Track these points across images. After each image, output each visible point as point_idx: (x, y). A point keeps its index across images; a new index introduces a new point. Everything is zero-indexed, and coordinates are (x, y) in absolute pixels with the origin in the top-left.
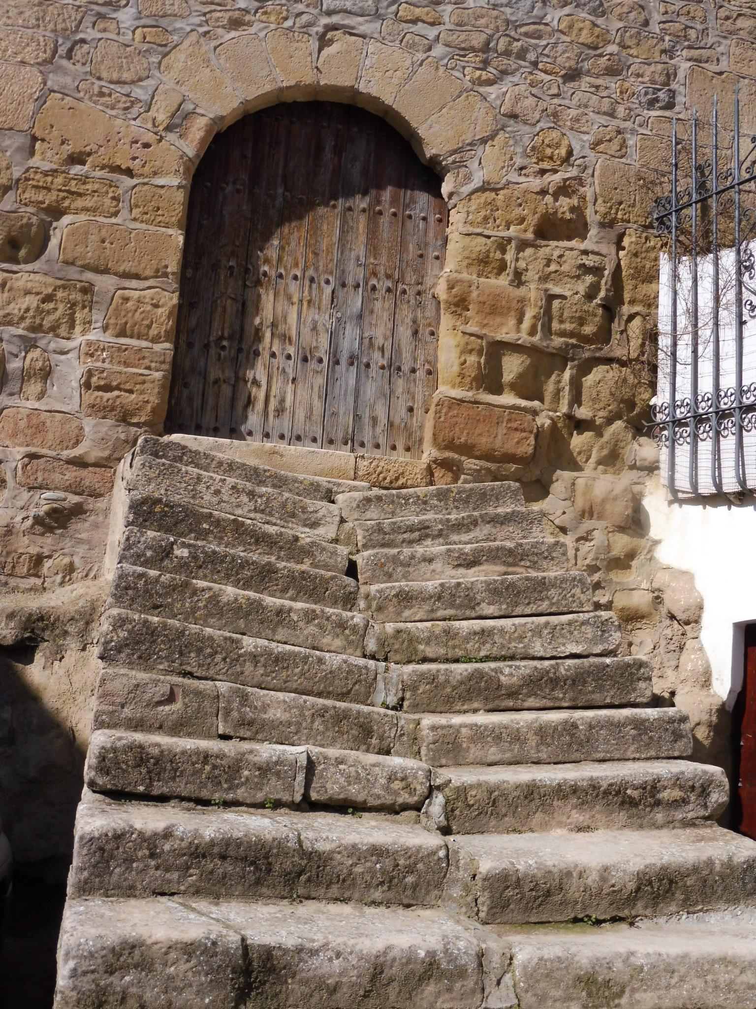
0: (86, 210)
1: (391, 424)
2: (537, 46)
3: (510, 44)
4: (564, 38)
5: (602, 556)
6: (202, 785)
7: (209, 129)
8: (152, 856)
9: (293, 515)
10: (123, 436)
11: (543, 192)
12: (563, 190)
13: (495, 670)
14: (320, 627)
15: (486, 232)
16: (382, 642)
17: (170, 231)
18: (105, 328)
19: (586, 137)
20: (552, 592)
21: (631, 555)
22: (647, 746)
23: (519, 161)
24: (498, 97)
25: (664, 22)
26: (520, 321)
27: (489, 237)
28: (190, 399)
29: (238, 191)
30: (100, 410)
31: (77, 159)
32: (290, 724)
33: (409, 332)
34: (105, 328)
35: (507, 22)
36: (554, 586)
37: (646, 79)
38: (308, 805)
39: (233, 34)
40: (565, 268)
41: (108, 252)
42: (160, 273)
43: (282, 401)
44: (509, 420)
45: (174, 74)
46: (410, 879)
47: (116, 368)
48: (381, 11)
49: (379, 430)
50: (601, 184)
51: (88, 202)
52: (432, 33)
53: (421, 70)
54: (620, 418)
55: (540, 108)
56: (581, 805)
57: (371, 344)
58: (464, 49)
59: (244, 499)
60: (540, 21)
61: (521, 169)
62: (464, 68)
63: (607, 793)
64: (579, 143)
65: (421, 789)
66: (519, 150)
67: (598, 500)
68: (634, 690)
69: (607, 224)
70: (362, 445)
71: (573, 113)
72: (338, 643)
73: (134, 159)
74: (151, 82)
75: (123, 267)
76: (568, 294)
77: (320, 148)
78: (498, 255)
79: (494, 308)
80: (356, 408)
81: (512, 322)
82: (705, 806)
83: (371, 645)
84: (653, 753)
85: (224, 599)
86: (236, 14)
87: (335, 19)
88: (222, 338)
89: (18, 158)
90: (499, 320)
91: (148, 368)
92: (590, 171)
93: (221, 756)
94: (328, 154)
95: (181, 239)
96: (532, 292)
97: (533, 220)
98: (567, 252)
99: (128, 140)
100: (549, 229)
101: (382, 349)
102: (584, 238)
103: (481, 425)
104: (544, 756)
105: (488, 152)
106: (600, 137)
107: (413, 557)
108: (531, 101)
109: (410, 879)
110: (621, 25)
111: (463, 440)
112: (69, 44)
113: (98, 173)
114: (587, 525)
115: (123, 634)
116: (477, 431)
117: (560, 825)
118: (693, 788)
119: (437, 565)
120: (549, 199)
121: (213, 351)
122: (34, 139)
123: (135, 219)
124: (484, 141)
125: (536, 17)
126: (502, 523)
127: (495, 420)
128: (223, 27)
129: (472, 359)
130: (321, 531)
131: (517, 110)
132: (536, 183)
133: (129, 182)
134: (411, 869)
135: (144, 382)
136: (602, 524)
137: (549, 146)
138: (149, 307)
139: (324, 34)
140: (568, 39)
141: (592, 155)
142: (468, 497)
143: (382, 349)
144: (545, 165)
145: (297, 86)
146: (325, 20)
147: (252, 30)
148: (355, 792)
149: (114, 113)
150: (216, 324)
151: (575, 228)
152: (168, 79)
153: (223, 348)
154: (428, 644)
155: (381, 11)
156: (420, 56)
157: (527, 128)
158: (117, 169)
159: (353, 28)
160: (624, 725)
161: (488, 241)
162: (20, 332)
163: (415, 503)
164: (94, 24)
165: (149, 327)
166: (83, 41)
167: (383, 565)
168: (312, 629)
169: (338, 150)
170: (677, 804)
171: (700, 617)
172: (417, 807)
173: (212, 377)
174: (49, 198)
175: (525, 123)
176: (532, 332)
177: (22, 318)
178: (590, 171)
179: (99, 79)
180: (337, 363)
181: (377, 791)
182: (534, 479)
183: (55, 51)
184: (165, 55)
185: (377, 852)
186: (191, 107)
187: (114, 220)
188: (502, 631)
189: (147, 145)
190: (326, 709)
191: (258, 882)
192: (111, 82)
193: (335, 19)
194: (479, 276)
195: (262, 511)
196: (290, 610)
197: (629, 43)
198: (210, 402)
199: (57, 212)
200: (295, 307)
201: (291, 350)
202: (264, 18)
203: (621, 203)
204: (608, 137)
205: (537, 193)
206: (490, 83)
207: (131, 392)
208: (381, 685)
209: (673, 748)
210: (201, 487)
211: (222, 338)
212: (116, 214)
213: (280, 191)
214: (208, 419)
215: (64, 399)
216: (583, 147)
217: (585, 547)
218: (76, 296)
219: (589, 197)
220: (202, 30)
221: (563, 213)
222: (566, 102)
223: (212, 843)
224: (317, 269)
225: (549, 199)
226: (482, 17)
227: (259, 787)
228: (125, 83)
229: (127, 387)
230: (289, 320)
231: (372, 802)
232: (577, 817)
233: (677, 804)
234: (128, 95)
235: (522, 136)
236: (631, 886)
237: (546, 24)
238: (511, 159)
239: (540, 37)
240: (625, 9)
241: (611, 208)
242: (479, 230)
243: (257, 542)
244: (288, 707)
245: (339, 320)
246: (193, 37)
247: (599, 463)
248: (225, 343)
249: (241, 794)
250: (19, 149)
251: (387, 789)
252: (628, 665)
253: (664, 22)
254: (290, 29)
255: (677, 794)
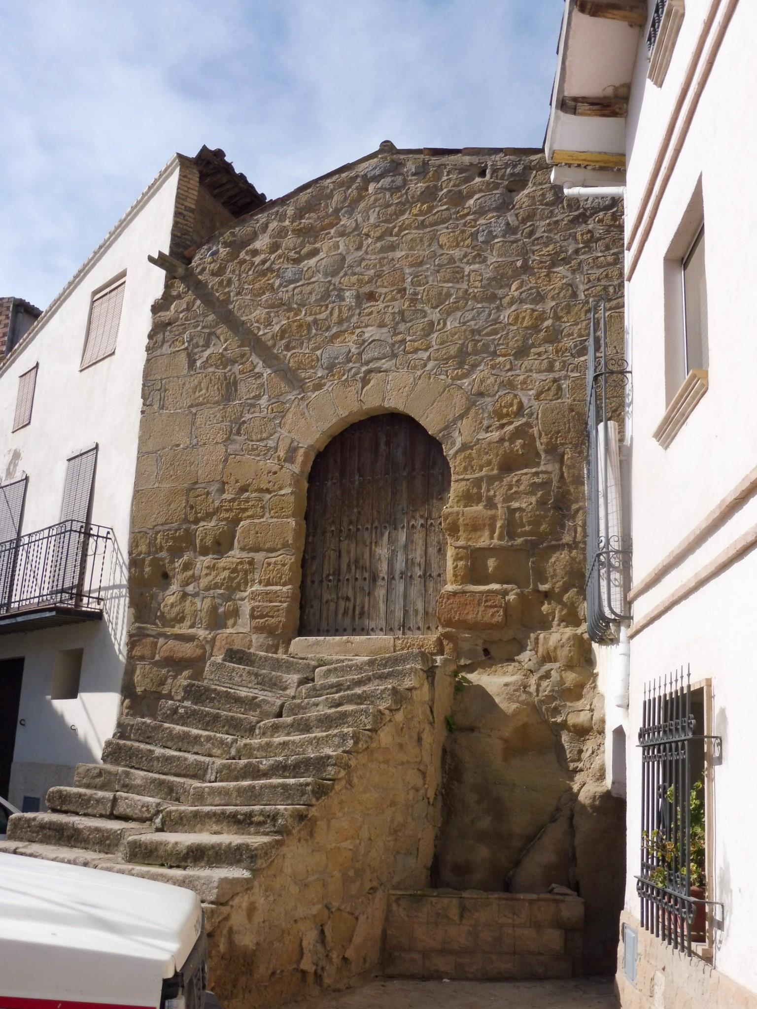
0: (249, 517)
1: (426, 613)
2: (494, 339)
3: (475, 345)
4: (512, 328)
5: (557, 688)
6: (78, 807)
7: (306, 455)
8: (29, 827)
9: (275, 685)
10: (271, 643)
11: (502, 440)
12: (519, 433)
13: (258, 762)
14: (213, 744)
15: (467, 477)
16: (238, 751)
17: (289, 520)
18: (260, 582)
19: (531, 393)
20: (350, 719)
21: (581, 686)
22: (288, 798)
23: (486, 423)
24: (469, 384)
25: (588, 290)
26: (492, 532)
27: (468, 480)
28: (314, 614)
29: (334, 484)
30: (258, 629)
31: (244, 489)
32: (141, 786)
33: (436, 550)
34: (260, 582)
35: (473, 332)
36: (351, 715)
37: (576, 335)
38: (112, 816)
39: (317, 393)
40: (522, 488)
41: (259, 539)
42: (285, 545)
43: (363, 608)
44: (486, 601)
45: (287, 427)
46: (108, 842)
47: (265, 604)
48: (396, 352)
49: (419, 618)
50: (543, 423)
51: (250, 513)
52: (425, 355)
53: (420, 382)
54: (574, 586)
55: (498, 382)
56: (218, 822)
57: (413, 563)
58: (446, 359)
59: (253, 678)
60: (496, 321)
61: (488, 427)
62: (447, 371)
63: (229, 816)
64: (526, 397)
65: (152, 811)
66: (486, 415)
67: (552, 648)
68: (325, 771)
69: (552, 450)
70: (409, 629)
71: (521, 378)
72: (219, 752)
73: (269, 482)
74: (277, 435)
75: (267, 546)
76: (524, 506)
77: (377, 445)
78: (475, 490)
79: (475, 527)
80: (405, 606)
81: (487, 533)
82: (274, 826)
83: (233, 752)
84: (290, 802)
85: (174, 732)
86: (317, 381)
87: (371, 365)
88: (329, 575)
89: (217, 496)
90: (479, 533)
91: (280, 602)
92: (535, 416)
93: (85, 795)
94: (383, 447)
95: (294, 523)
96: (500, 511)
97: (496, 461)
98: (525, 476)
99: (265, 473)
100: (508, 466)
101: (419, 565)
102: (538, 464)
103: (468, 607)
104: (238, 802)
105: (466, 425)
106: (540, 389)
107: (308, 704)
108: (492, 379)
109: (108, 842)
110: (554, 303)
111: (456, 618)
112: (238, 426)
113: (254, 495)
114: (548, 666)
115: (110, 749)
116: (466, 612)
117: (208, 830)
118: (269, 816)
119: (320, 707)
120: (507, 444)
121: (325, 583)
122: (224, 483)
123: (272, 517)
124: (461, 417)
125: (493, 320)
126: (386, 678)
127: (476, 602)
128: (311, 391)
129: (461, 564)
130: (288, 692)
131: (482, 389)
132: (495, 435)
133: (268, 496)
134: (108, 838)
135: (278, 610)
136: (557, 665)
137: (505, 407)
138: (279, 567)
139: (365, 377)
140: (515, 328)
141: (535, 403)
142: (387, 662)
143: (419, 565)
144: (504, 421)
145: (350, 414)
146: (364, 369)
147: (326, 388)
148: (129, 812)
149: (259, 458)
150: (326, 568)
151: (529, 458)
152: (284, 432)
153: (330, 581)
154: (258, 751)
155: (396, 352)
156: (419, 373)
157: (490, 399)
158: (261, 491)
159: (381, 368)
160: (278, 787)
161: (468, 483)
162: (222, 591)
163: (355, 670)
164: (249, 410)
165: (281, 578)
166: (244, 422)
167: (293, 709)
168: (209, 745)
169: (388, 443)
170: (261, 824)
171: (604, 729)
172: (150, 819)
173: (325, 599)
174: (231, 515)
175: (489, 395)
176: (501, 538)
177: (222, 584)
178: (535, 416)
179: (252, 441)
180: (393, 578)
181: (137, 811)
182: (511, 637)
183: (231, 432)
184: (283, 417)
185: (97, 830)
186: (296, 444)
187: (262, 520)
188: (294, 742)
189: (275, 473)
190: (155, 779)
191: (60, 839)
192: (258, 441)
193: (371, 365)
194: (465, 507)
195: (261, 684)
196: (201, 736)
197: (561, 314)
198: (324, 615)
199: (236, 521)
200: (368, 548)
201: (366, 575)
202: (331, 378)
203: (559, 432)
204: (546, 388)
205: (497, 442)
206: (465, 376)
207: (273, 617)
208: (209, 771)
209: (300, 800)
210: (234, 674)
211: (329, 575)
212: (262, 517)
213: (357, 477)
214: (324, 625)
215: (243, 626)
216: (530, 400)
217: (545, 684)
218: (246, 566)
219: (536, 435)
220: (299, 397)
221: (517, 450)
222: (518, 372)
223: (46, 823)
224: (379, 521)
225: (507, 444)
226: (456, 334)
227: (95, 808)
228: (264, 439)
229: (270, 614)
230: (365, 557)
231: (135, 816)
232: (215, 828)
233: (261, 824)
234: (266, 446)
235: (487, 405)
236: (185, 851)
237: (500, 323)
238: (481, 423)
239: (497, 334)
240: (557, 291)
241: (551, 438)
242: (462, 477)
243: (235, 702)
244: (143, 778)
245: (393, 551)
246: (296, 402)
247: (562, 620)
248: (331, 578)
249: (90, 811)
250: (218, 490)
251: (140, 811)
252: (322, 758)
253: (588, 290)
254: (346, 380)
255: (261, 818)
